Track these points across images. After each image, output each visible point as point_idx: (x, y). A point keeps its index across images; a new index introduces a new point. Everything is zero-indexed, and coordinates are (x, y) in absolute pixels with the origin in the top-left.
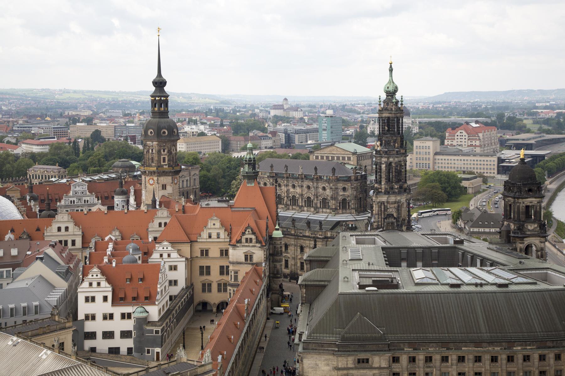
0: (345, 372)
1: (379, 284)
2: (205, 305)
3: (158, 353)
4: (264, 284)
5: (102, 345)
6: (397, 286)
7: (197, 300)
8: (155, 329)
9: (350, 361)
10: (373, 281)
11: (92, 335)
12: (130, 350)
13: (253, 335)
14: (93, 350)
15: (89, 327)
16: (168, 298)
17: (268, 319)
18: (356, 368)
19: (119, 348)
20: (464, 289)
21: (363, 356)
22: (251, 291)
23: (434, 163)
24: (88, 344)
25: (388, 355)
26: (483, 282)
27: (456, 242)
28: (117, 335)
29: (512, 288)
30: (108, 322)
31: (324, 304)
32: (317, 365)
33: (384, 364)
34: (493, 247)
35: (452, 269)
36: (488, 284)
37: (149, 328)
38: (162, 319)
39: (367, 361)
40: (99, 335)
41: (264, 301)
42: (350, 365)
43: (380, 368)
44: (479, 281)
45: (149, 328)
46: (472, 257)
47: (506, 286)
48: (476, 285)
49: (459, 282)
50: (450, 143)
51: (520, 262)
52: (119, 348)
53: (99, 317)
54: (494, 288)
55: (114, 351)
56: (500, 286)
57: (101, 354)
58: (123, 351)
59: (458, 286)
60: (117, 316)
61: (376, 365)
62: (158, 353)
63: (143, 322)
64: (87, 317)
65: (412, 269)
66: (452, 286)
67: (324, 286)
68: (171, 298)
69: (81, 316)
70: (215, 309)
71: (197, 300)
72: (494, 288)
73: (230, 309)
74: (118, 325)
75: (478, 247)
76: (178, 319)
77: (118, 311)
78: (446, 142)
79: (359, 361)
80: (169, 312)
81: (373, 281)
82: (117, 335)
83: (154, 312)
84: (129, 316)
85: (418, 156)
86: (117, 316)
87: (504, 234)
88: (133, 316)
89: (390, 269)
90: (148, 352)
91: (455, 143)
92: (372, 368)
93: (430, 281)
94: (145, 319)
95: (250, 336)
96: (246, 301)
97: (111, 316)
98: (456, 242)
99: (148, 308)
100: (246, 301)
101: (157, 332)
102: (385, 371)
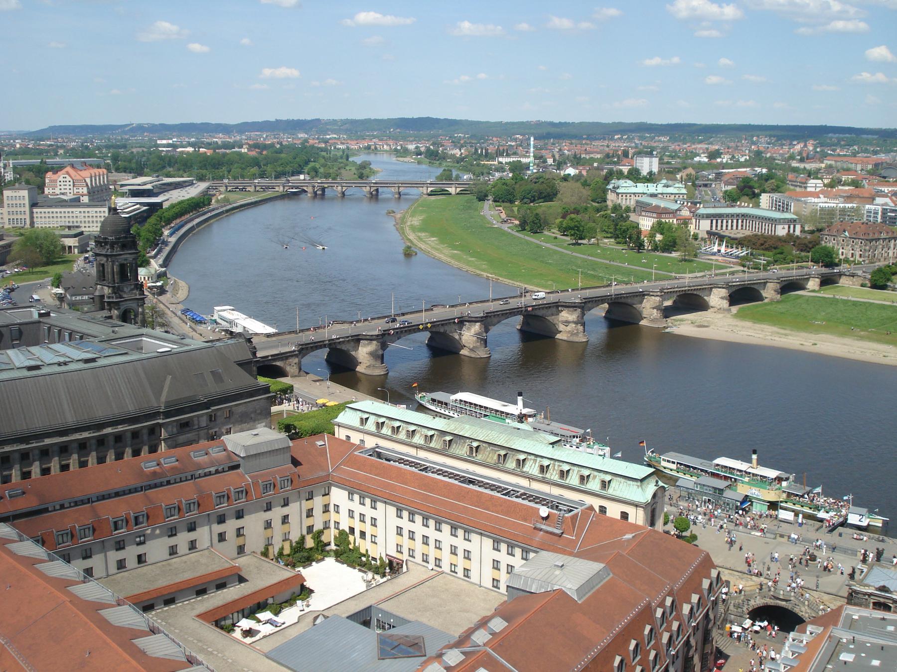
20: (45, 370)
23: (32, 218)
26: (68, 360)
27: (41, 315)
29: (102, 362)
34: (86, 316)
44: (62, 360)
46: (60, 331)
47: (93, 360)
48: (59, 364)
49: (40, 363)
50: (51, 191)
51: (113, 332)
56: (87, 361)
59: (37, 368)
66: (30, 368)
72: (81, 366)
75: (70, 320)
78: (46, 191)
85: (11, 210)
87: (97, 299)
91: (57, 191)
98: (41, 315)
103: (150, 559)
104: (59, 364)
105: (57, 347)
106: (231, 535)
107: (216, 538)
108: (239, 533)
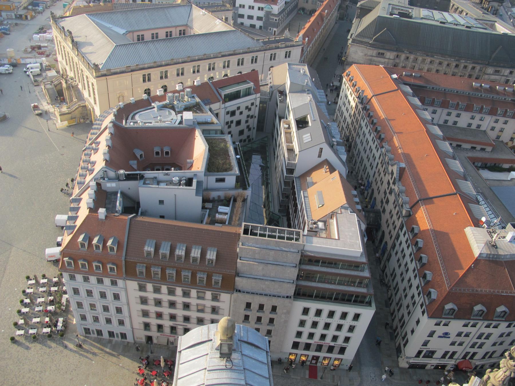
0: (370, 58)
1: (401, 15)
2: (303, 9)
3: (275, 31)
4: (338, 3)
5: (247, 22)
6: (411, 17)
7: (300, 6)
8: (275, 18)
9: (374, 52)
10: (399, 12)
11: (242, 16)
12: (261, 27)
13: (326, 30)
14: (242, 24)
15: (241, 11)
16: (284, 2)
17: (336, 23)
18: (376, 57)
19: (255, 25)
21: (381, 51)
22: (330, 6)
24: (240, 20)
25: (395, 53)
28: (255, 18)
29: (473, 30)
30: (251, 10)
31: (368, 19)
32: (357, 52)
33: (392, 57)
35: (443, 13)
36: (460, 25)
37: (271, 17)
38: (280, 13)
39: (383, 54)
40: (246, 17)
41: (336, 14)
42: (374, 55)
43: (389, 59)
44: (456, 23)
45: (271, 17)
48: (455, 24)
49: (445, 21)
52: (255, 25)
53: (247, 7)
54: (464, 28)
55: (253, 26)
56: (467, 27)
57: (246, 27)
58: (258, 27)
59: (444, 23)
60: (256, 8)
61: (387, 57)
62: (275, 31)
63: (268, 14)
64: (240, 6)
65: (421, 9)
67: (371, 10)
68: (286, 2)
69: (237, 5)
70: (308, 13)
71: (300, 6)
73: (317, 13)
74: (256, 13)
76: (288, 14)
77: (257, 5)
79: (379, 53)
80: (283, 10)
81: (399, 12)
82: (255, 18)
83: (276, 9)
84: (262, 9)
86: (256, 8)
88: (264, 9)
89: (410, 7)
90: (270, 30)
92: (385, 58)
93: (430, 18)
94: (270, 12)
95: (325, 31)
96: (326, 11)
97: (253, 8)
99: (273, 6)
100: (326, 11)
101: (276, 20)
102: (392, 61)
103: (458, 125)
104: (455, 24)
105: (456, 16)
106: (497, 129)
107: (490, 128)
108: (502, 130)
